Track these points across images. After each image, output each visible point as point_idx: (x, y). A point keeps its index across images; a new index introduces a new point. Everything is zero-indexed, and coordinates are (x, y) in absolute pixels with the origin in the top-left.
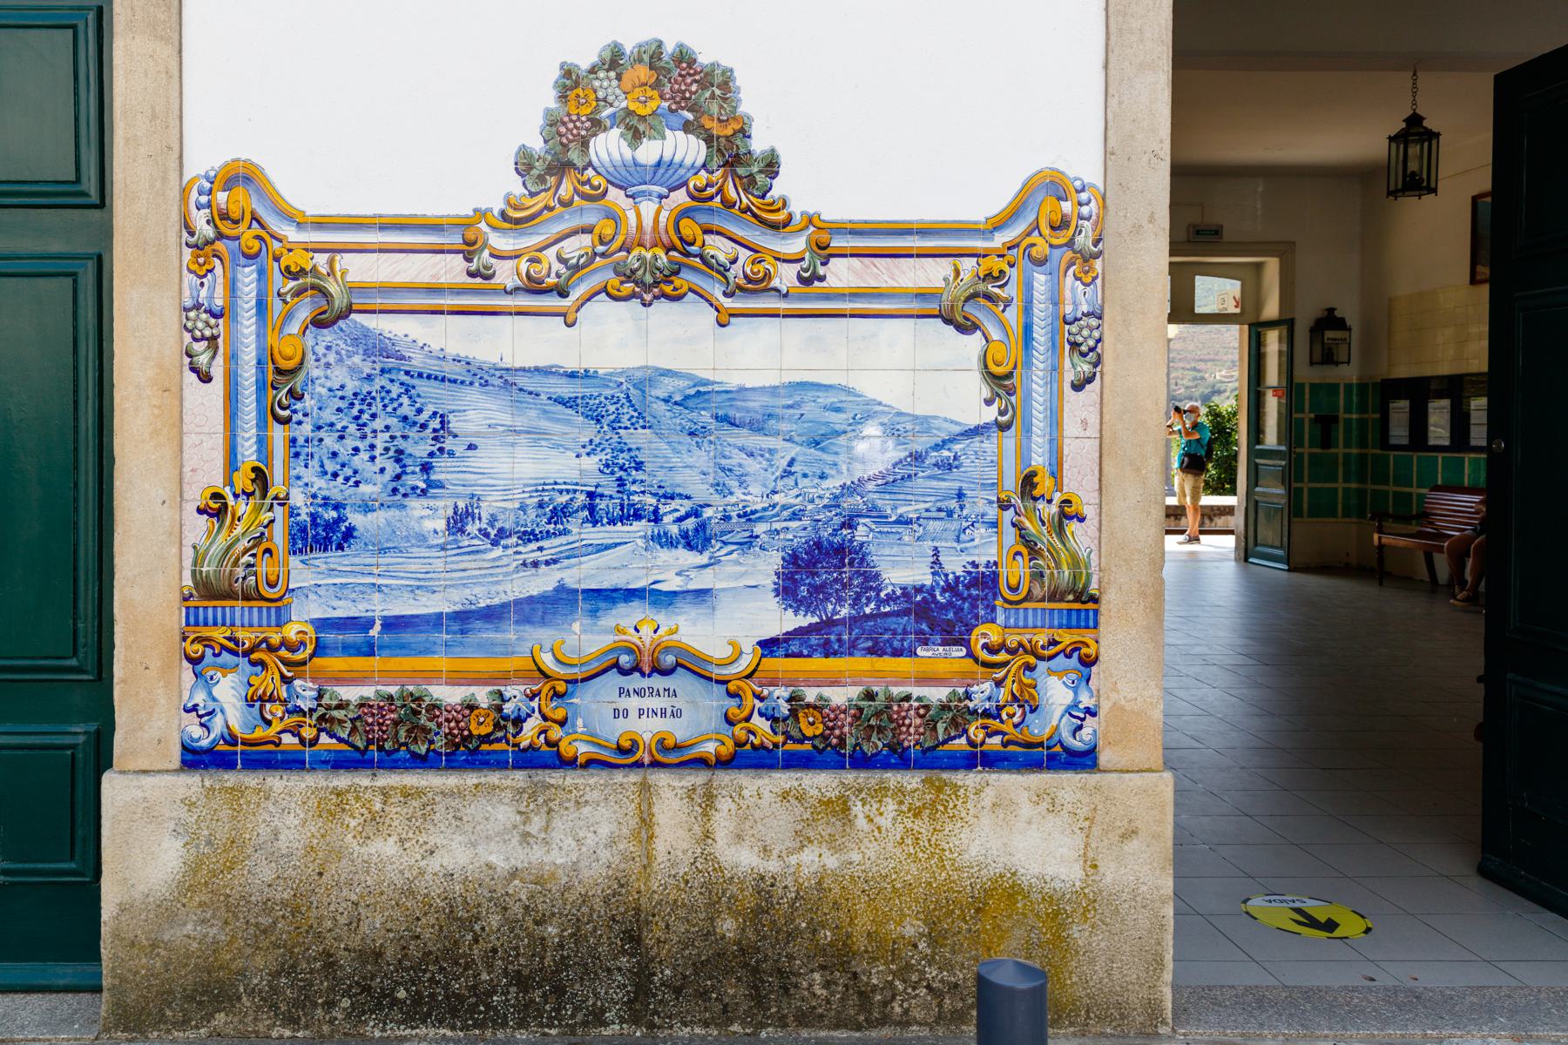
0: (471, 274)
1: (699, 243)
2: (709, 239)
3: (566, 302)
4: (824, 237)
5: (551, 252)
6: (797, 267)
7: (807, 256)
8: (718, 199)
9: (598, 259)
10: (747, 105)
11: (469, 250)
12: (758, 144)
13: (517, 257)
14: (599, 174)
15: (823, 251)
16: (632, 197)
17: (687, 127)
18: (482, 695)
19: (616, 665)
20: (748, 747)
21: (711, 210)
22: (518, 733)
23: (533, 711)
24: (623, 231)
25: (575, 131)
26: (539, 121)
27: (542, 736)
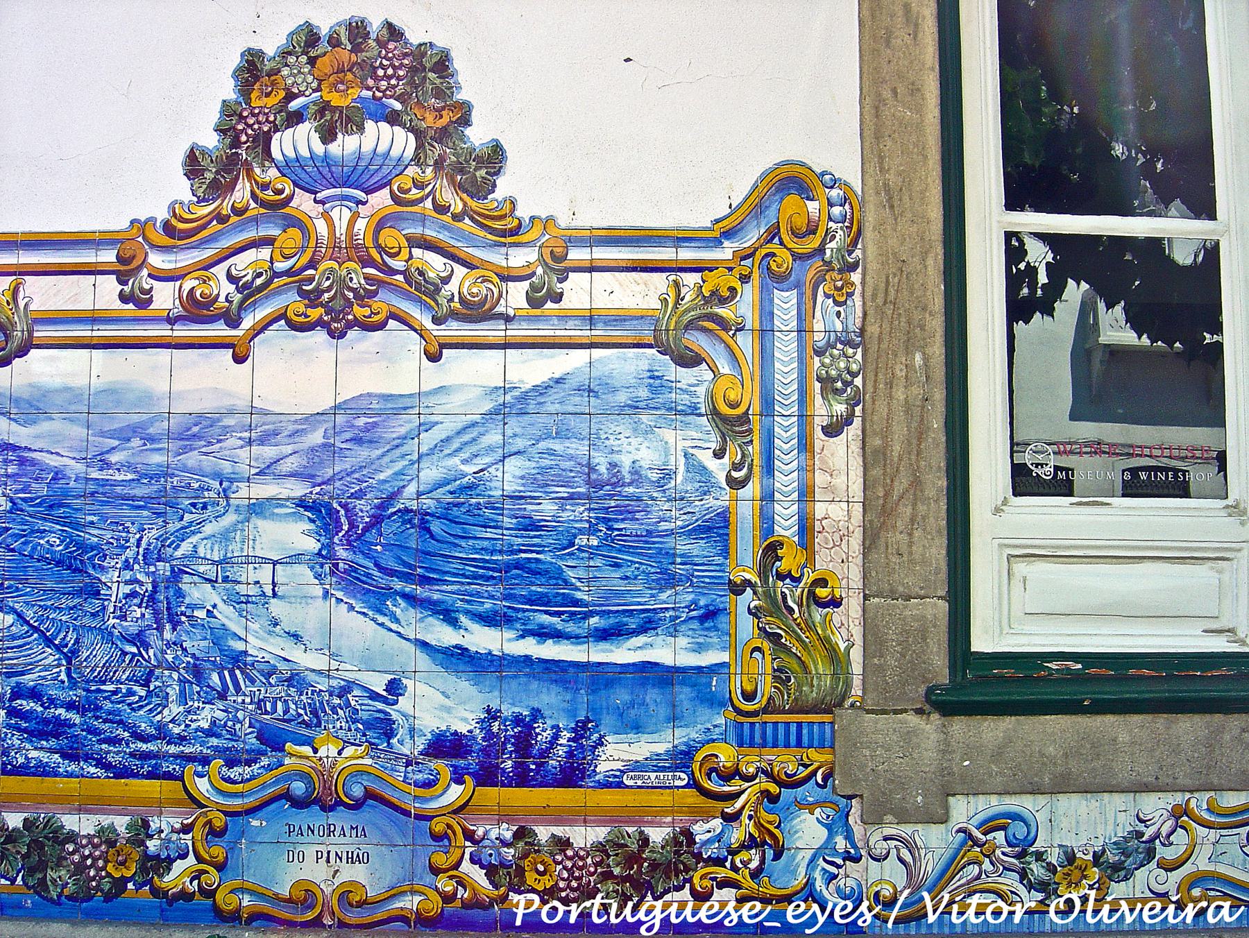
0: (124, 298)
1: (405, 254)
2: (417, 252)
5: (220, 271)
6: (525, 285)
7: (540, 271)
11: (125, 269)
12: (477, 135)
13: (182, 277)
14: (284, 175)
16: (323, 202)
17: (393, 119)
19: (287, 796)
20: (458, 903)
21: (423, 219)
25: (256, 126)
26: (214, 116)
27: (195, 883)
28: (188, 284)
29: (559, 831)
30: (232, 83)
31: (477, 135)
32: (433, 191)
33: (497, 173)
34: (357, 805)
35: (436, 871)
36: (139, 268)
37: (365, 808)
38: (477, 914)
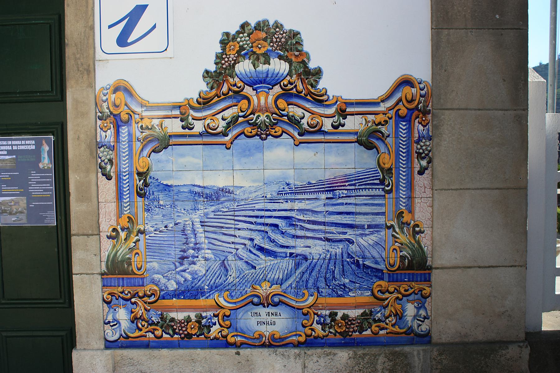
0: (183, 128)
3: (227, 139)
4: (344, 107)
5: (219, 116)
6: (331, 120)
8: (295, 89)
9: (240, 119)
10: (306, 47)
12: (312, 65)
13: (205, 119)
15: (343, 113)
17: (280, 57)
18: (193, 315)
19: (252, 303)
20: (312, 337)
22: (209, 332)
23: (216, 322)
24: (252, 106)
28: (208, 121)
29: (346, 312)
30: (219, 45)
31: (312, 65)
32: (296, 86)
33: (319, 78)
34: (276, 305)
35: (304, 326)
36: (188, 115)
37: (279, 307)
38: (319, 340)
